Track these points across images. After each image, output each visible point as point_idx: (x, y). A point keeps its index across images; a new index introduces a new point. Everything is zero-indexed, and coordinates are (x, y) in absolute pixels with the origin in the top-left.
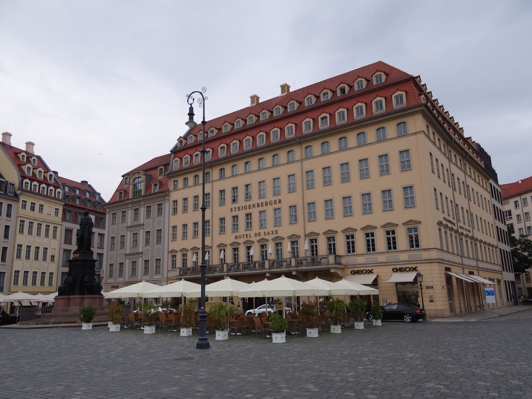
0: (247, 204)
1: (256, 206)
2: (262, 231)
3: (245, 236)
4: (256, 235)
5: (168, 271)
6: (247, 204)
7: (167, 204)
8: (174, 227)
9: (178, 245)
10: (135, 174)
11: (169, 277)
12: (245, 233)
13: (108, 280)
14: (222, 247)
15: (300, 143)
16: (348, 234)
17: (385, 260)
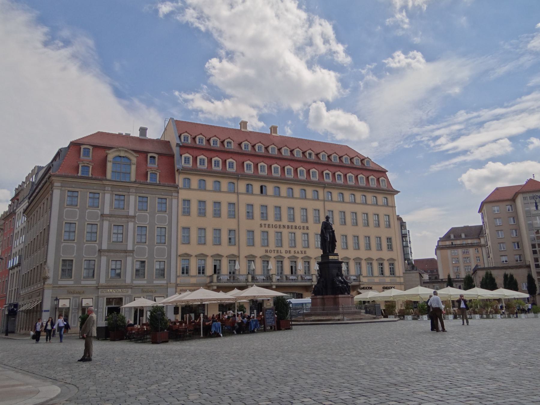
0: (278, 223)
1: (286, 227)
2: (292, 250)
3: (276, 252)
4: (286, 252)
5: (177, 277)
6: (278, 223)
7: (174, 201)
8: (187, 229)
9: (193, 249)
10: (120, 150)
11: (178, 282)
12: (276, 249)
13: (61, 283)
14: (251, 259)
15: (324, 188)
16: (357, 261)
17: (378, 281)
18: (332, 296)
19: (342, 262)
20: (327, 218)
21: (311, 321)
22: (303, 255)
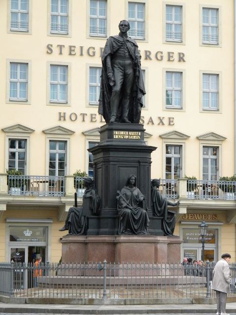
3: (88, 118)
18: (107, 238)
19: (152, 149)
20: (124, 27)
21: (32, 301)
22: (166, 129)
